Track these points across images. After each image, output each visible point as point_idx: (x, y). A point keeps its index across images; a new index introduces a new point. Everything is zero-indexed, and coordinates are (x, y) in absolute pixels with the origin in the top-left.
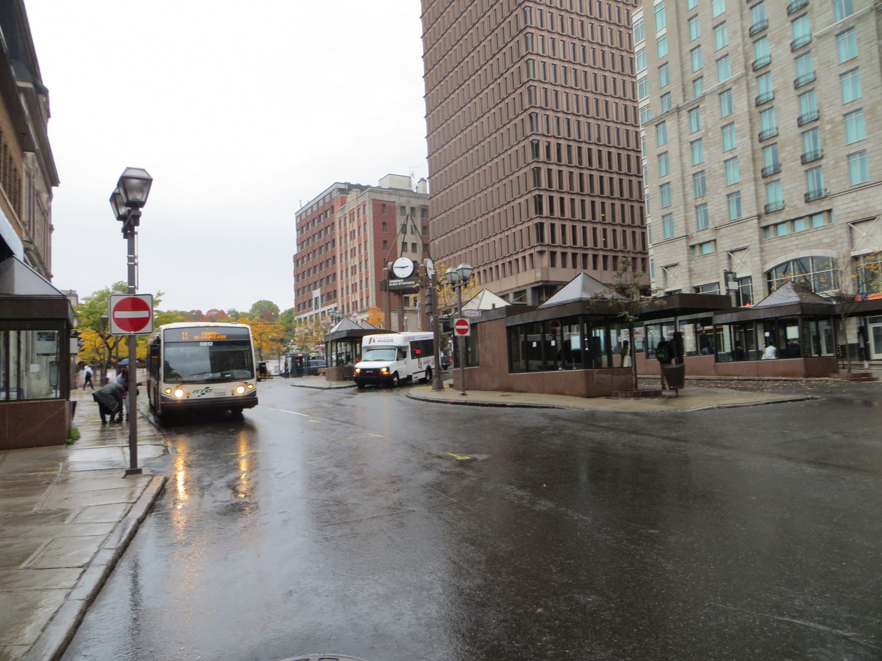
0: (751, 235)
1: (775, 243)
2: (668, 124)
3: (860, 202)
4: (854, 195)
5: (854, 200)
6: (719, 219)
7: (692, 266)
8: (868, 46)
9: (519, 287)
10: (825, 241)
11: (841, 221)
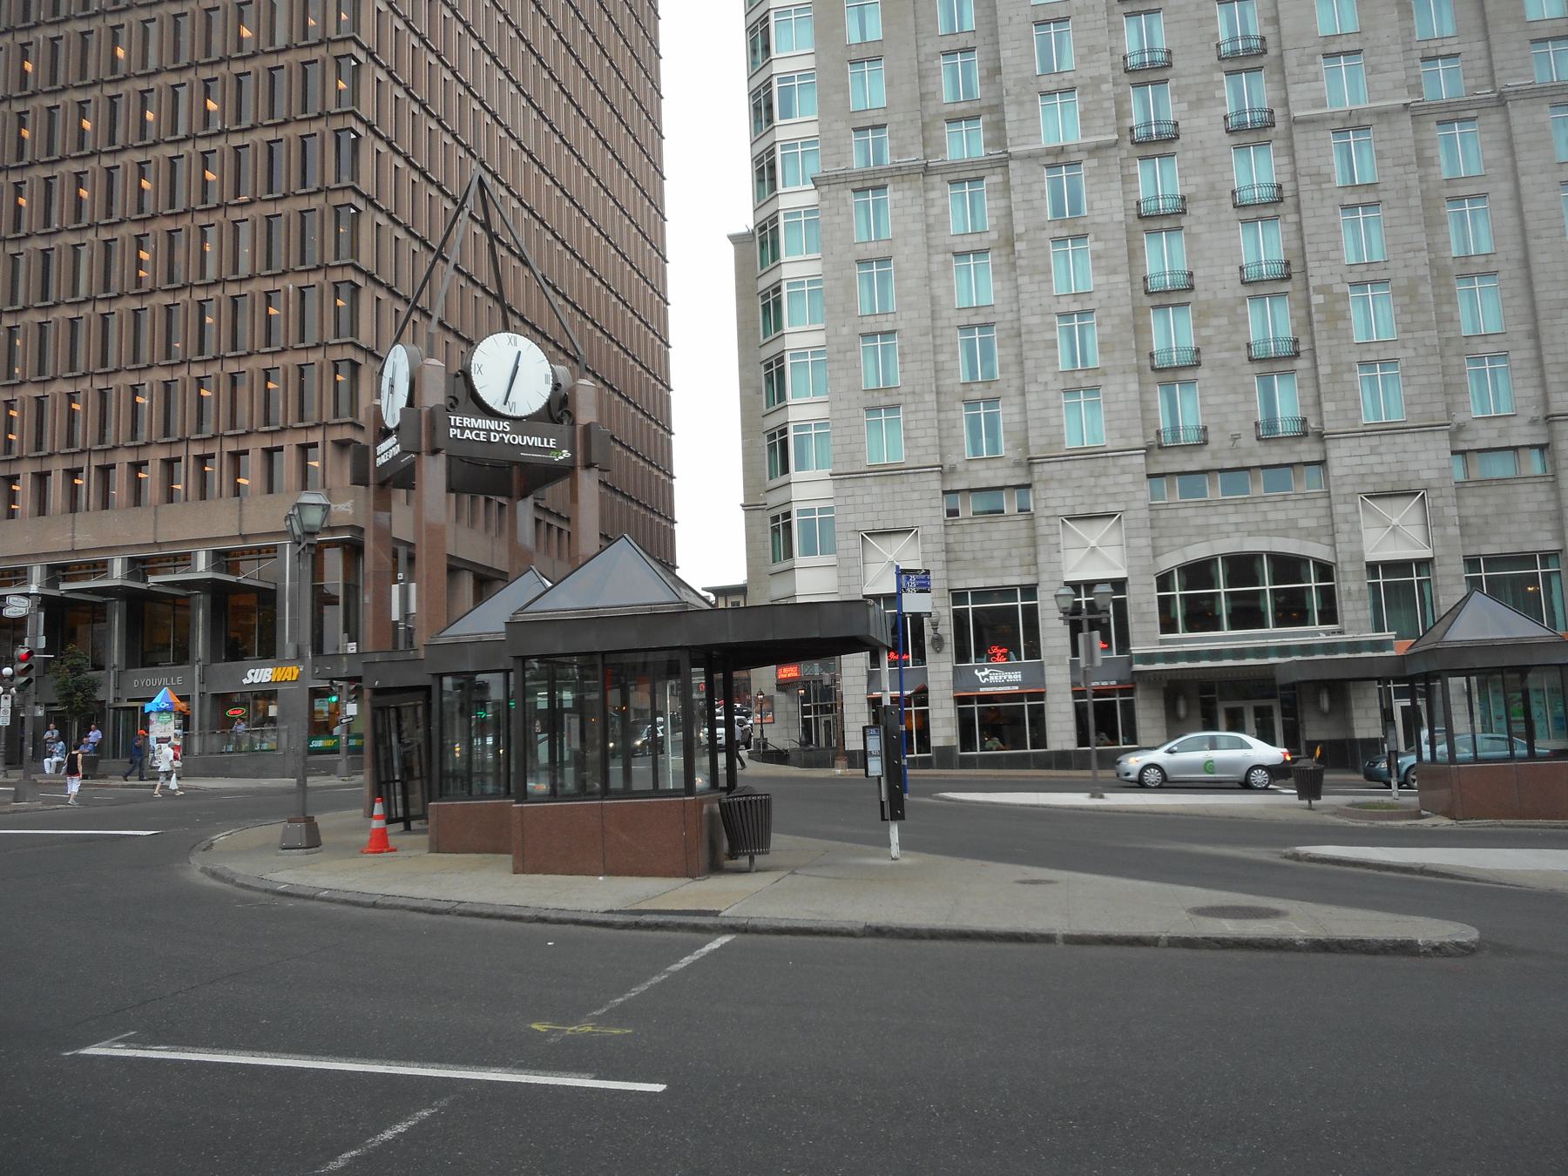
0: (1131, 488)
1: (1182, 513)
2: (890, 195)
3: (1387, 458)
4: (1374, 441)
5: (1373, 451)
6: (1043, 441)
7: (951, 539)
8: (1400, 170)
9: (244, 537)
10: (1303, 523)
11: (1348, 490)
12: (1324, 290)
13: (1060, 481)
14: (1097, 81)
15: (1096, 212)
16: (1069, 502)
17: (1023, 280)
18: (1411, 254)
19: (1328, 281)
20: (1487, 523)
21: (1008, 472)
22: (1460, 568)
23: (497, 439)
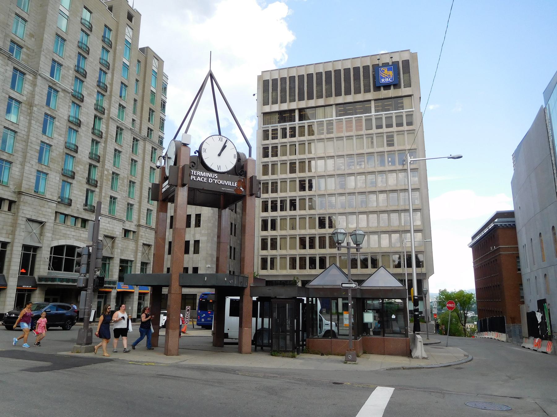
0: (50, 214)
3: (111, 226)
4: (109, 220)
6: (27, 187)
12: (108, 170)
13: (29, 204)
14: (68, 68)
15: (59, 112)
16: (31, 213)
17: (33, 122)
18: (125, 170)
19: (109, 168)
20: (123, 250)
21: (9, 194)
22: (118, 262)
23: (212, 182)
